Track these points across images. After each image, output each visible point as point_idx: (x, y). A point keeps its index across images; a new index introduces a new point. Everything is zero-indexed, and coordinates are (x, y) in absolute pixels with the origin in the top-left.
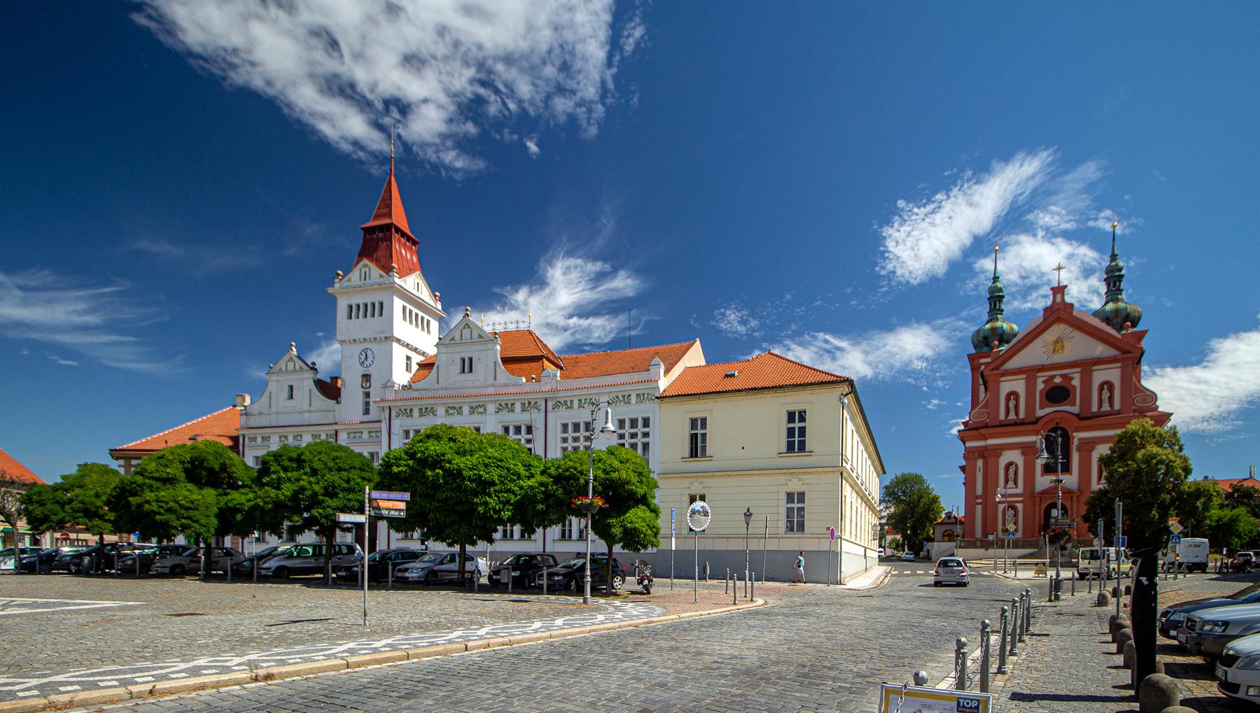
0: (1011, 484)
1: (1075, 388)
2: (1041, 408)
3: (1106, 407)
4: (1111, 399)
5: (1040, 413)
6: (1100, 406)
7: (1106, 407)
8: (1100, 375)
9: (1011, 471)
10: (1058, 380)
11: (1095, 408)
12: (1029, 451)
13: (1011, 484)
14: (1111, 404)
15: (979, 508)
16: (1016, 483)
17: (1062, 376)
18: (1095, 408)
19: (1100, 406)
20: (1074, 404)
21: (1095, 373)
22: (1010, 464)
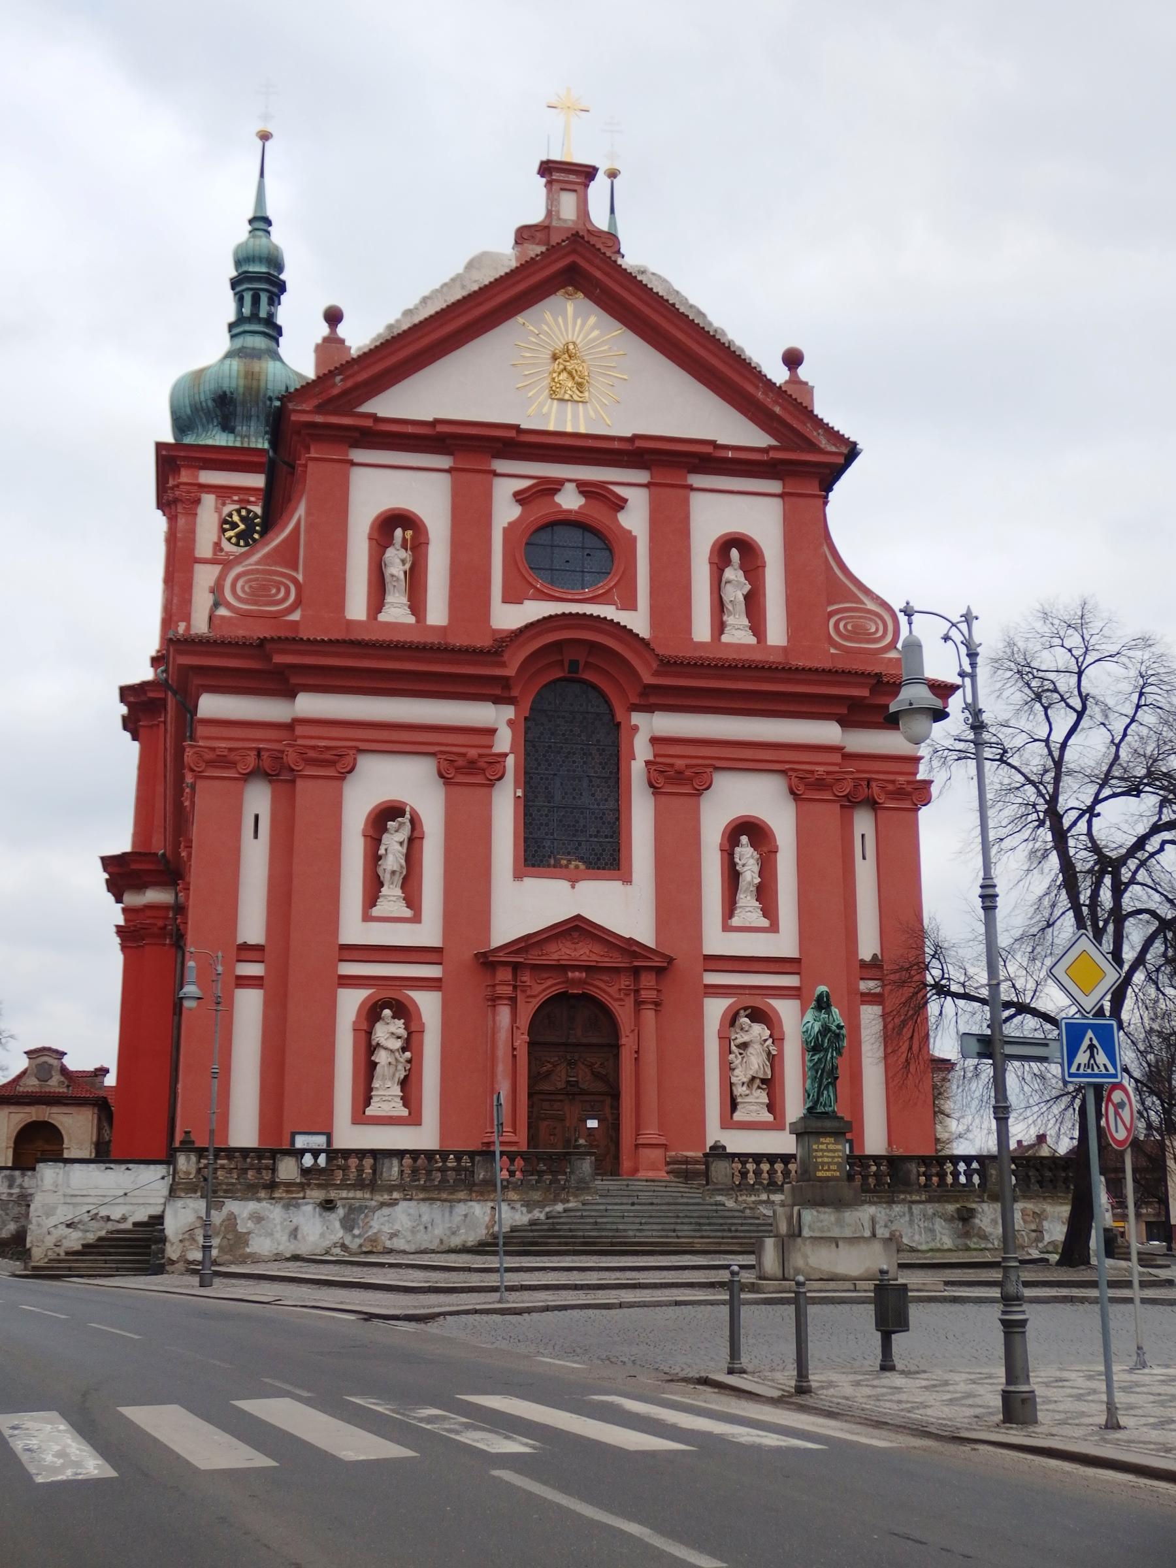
0: (391, 900)
1: (630, 540)
2: (512, 597)
3: (738, 633)
4: (754, 603)
5: (509, 617)
6: (719, 627)
7: (738, 633)
8: (722, 511)
9: (394, 843)
10: (570, 501)
11: (702, 631)
12: (464, 767)
13: (391, 900)
14: (757, 624)
15: (249, 1006)
16: (412, 899)
17: (585, 488)
18: (702, 631)
19: (719, 627)
20: (630, 604)
21: (696, 499)
22: (386, 815)
